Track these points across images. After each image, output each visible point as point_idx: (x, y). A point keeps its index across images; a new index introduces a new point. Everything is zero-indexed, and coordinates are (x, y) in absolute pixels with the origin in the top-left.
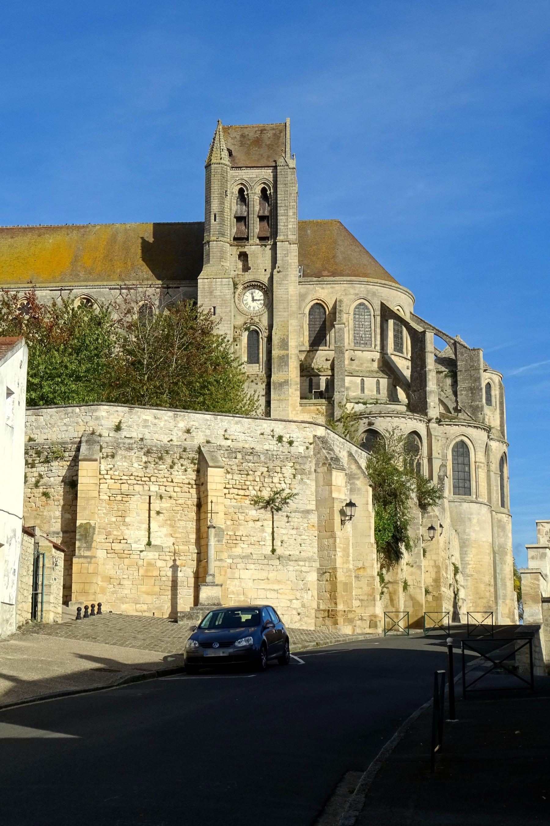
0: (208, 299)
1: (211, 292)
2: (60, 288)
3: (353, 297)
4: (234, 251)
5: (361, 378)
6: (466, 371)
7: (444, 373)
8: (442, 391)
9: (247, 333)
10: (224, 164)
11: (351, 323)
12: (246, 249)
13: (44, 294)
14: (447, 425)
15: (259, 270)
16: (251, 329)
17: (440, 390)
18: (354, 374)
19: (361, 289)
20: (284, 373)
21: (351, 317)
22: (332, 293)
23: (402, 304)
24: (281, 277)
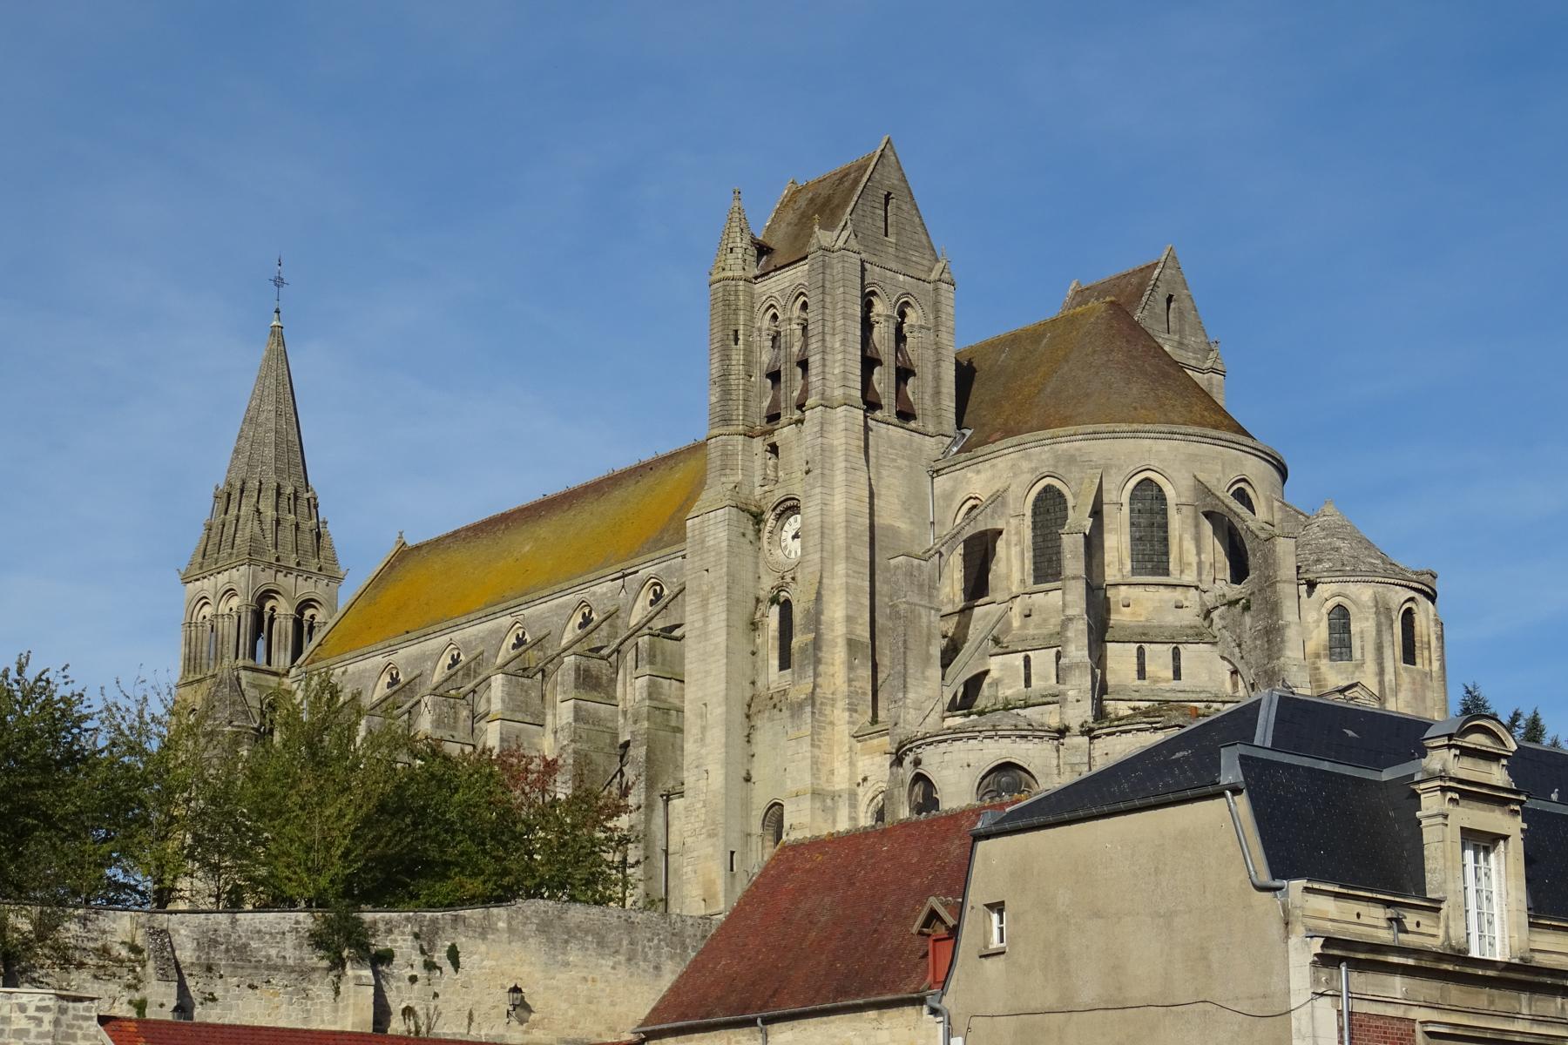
0: (699, 558)
1: (703, 542)
2: (620, 574)
3: (1028, 478)
4: (759, 445)
5: (1023, 654)
6: (1259, 591)
7: (1241, 603)
8: (1239, 645)
9: (776, 609)
10: (728, 279)
11: (1028, 534)
12: (775, 438)
13: (604, 590)
14: (1108, 734)
15: (793, 476)
16: (782, 600)
17: (1233, 644)
18: (1010, 649)
19: (1043, 457)
20: (807, 680)
21: (1028, 520)
22: (994, 477)
23: (1154, 464)
24: (811, 481)
